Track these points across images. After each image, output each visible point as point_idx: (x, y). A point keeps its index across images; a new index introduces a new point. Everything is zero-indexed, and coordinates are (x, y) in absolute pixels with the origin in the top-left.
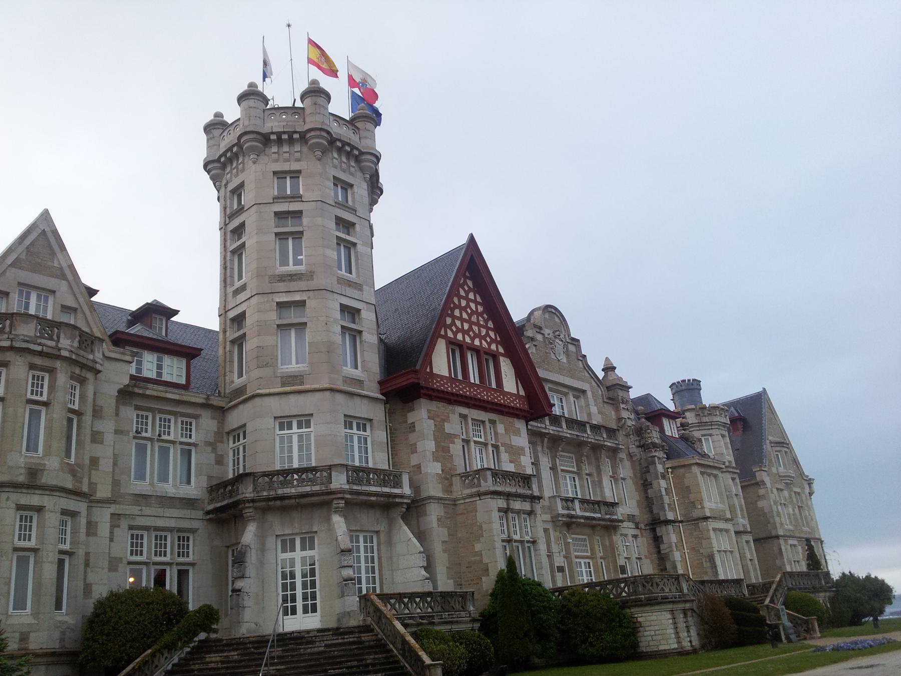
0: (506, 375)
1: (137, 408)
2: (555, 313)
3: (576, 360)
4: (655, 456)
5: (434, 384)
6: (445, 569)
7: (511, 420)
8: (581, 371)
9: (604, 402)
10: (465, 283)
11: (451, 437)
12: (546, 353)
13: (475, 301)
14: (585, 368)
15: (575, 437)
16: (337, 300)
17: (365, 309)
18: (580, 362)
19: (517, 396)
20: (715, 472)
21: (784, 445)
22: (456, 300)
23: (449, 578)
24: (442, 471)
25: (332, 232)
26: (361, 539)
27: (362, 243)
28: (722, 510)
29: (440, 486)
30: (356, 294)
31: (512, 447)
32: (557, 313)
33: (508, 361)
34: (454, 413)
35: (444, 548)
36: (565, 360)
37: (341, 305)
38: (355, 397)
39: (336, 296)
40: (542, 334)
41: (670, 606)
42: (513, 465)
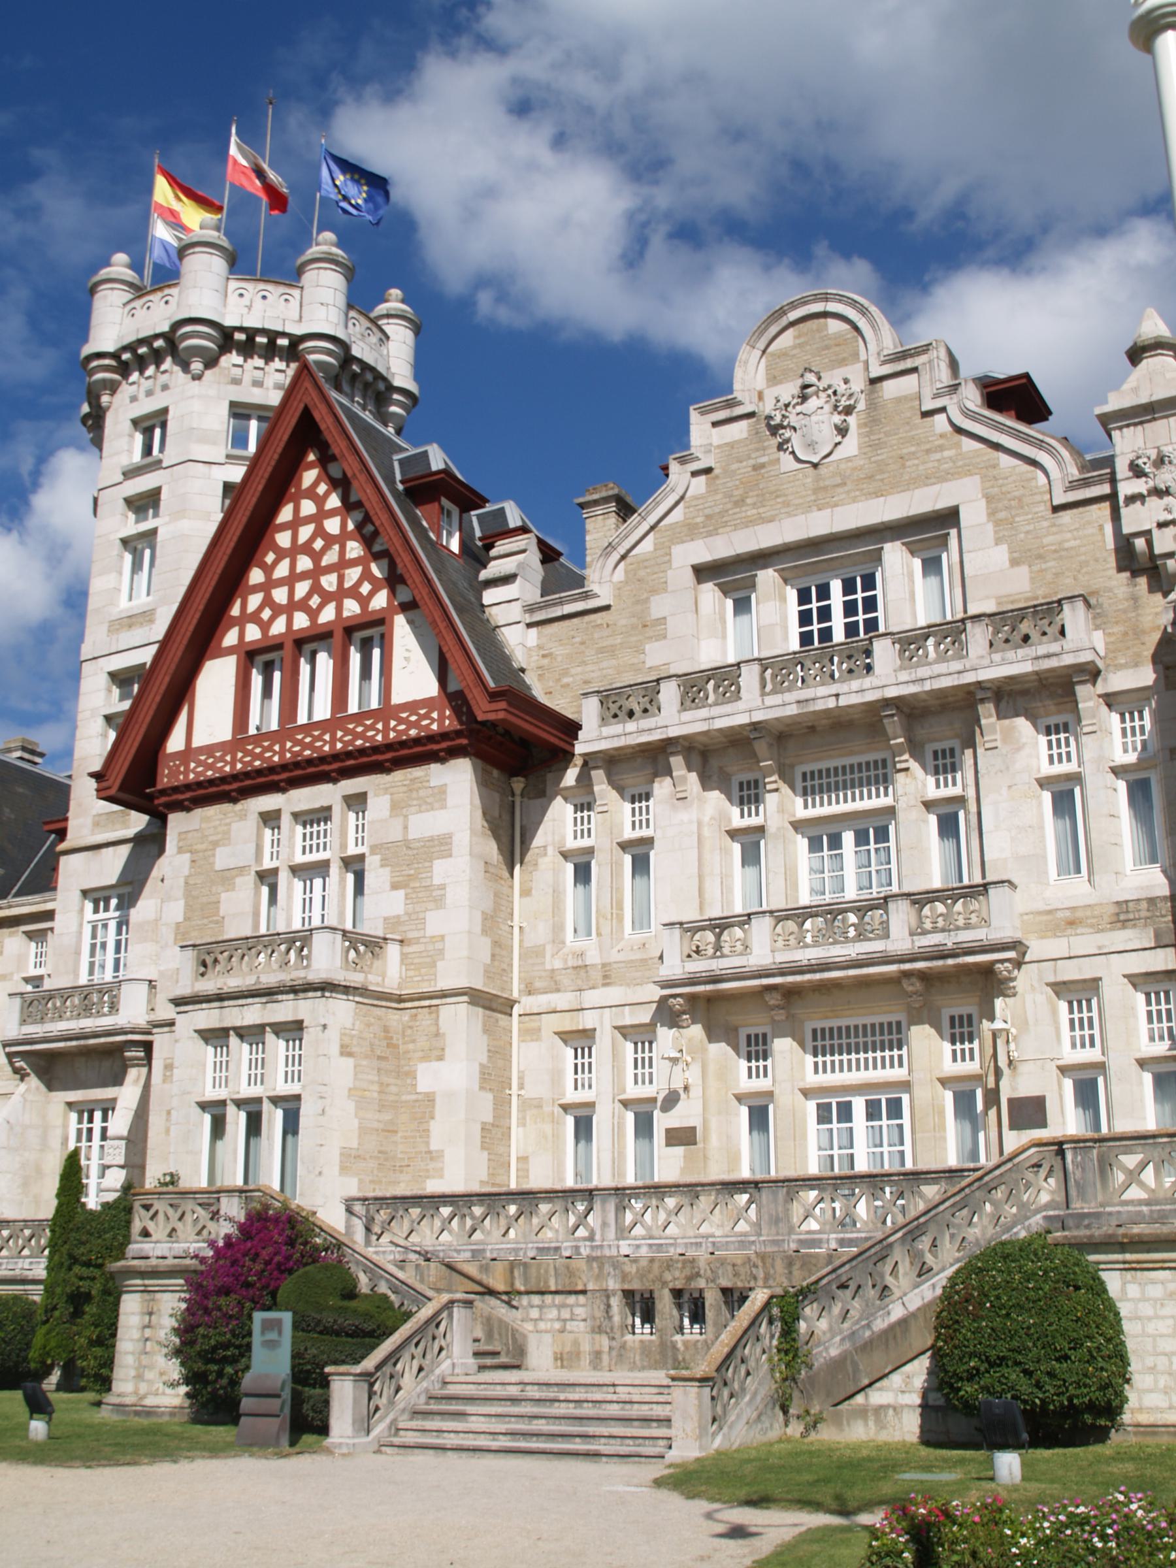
0: (407, 659)
2: (825, 315)
3: (917, 419)
7: (417, 772)
8: (941, 448)
9: (1056, 509)
11: (227, 877)
12: (756, 468)
14: (959, 430)
15: (792, 710)
18: (940, 419)
27: (167, 519)
31: (407, 843)
32: (833, 307)
34: (243, 816)
40: (751, 415)
42: (401, 893)
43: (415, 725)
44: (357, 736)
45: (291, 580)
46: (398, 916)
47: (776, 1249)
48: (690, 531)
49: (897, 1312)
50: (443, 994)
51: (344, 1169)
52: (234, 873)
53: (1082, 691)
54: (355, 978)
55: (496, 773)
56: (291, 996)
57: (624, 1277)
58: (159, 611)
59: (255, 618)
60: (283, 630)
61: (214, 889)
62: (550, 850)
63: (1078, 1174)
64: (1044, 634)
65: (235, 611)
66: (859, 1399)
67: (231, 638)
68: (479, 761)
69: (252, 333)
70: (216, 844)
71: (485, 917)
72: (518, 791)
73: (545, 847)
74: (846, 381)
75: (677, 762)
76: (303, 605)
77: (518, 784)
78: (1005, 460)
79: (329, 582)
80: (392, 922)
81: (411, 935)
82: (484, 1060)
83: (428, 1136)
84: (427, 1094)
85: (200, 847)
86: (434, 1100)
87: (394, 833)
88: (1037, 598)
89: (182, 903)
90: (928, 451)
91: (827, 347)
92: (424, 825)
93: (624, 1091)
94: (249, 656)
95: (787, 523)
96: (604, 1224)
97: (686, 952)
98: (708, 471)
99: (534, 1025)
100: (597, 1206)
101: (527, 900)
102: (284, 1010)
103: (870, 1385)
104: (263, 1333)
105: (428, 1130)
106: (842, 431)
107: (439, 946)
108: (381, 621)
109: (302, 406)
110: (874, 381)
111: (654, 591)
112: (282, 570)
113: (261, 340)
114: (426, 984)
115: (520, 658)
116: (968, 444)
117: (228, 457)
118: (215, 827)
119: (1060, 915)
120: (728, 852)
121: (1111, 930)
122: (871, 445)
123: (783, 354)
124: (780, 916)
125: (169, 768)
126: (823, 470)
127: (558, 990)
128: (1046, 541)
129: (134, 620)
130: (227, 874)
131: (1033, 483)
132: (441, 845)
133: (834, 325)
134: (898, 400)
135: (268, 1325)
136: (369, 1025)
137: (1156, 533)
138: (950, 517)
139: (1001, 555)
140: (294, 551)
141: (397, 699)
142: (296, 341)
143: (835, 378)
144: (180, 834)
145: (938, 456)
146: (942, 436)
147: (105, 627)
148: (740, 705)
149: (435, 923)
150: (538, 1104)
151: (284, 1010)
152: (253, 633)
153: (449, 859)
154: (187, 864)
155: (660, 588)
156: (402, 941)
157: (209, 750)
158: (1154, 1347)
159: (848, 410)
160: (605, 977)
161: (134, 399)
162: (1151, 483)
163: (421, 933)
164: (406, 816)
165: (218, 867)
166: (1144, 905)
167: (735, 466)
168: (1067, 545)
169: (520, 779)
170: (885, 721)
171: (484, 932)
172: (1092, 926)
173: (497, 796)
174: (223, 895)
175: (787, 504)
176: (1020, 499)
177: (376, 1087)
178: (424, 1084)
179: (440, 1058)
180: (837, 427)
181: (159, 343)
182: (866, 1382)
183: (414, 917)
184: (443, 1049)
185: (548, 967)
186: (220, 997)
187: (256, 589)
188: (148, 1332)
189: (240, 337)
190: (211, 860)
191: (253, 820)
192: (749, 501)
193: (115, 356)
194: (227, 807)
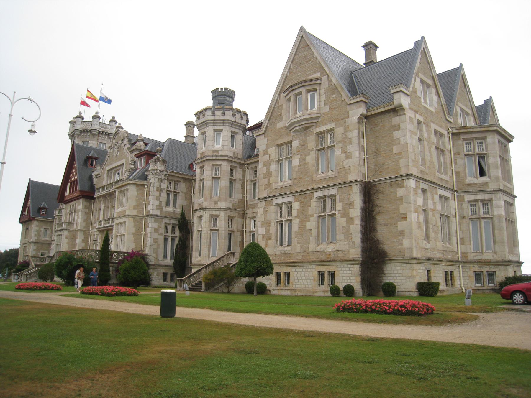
20: (126, 188)
21: (293, 88)
48: (108, 165)
55: (88, 200)
68: (85, 199)
69: (84, 130)
71: (84, 220)
77: (93, 201)
80: (76, 220)
82: (83, 238)
95: (114, 164)
98: (109, 156)
115: (94, 183)
122: (119, 153)
132: (79, 211)
138: (123, 164)
142: (90, 130)
148: (105, 191)
171: (84, 222)
173: (89, 203)
189: (82, 131)
193: (71, 134)
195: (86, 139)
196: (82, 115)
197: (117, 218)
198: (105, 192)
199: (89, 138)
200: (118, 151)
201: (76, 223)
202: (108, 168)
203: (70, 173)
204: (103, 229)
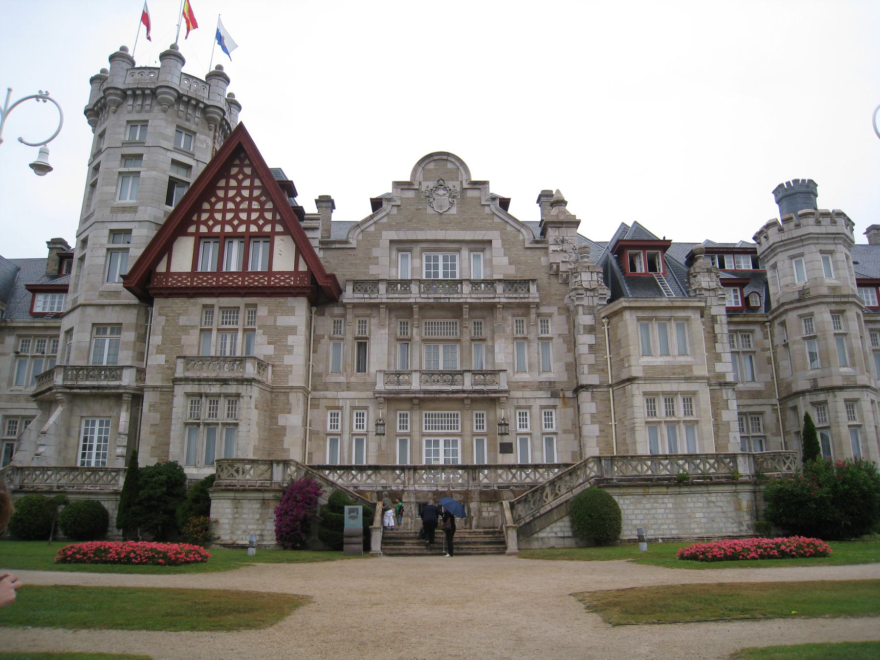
0: (280, 254)
1: (19, 336)
2: (447, 160)
4: (578, 305)
5: (167, 281)
6: (150, 448)
7: (282, 300)
8: (487, 219)
10: (241, 171)
11: (185, 329)
12: (417, 209)
13: (251, 188)
14: (494, 214)
16: (106, 227)
17: (137, 227)
18: (487, 208)
19: (296, 273)
22: (221, 193)
23: (152, 456)
24: (166, 361)
25: (114, 170)
26: (97, 423)
28: (685, 366)
29: (160, 376)
30: (128, 216)
31: (276, 327)
33: (288, 239)
35: (152, 430)
36: (454, 211)
37: (111, 231)
38: (107, 307)
39: (106, 224)
41: (232, 495)
43: (284, 281)
44: (255, 281)
45: (224, 211)
46: (271, 355)
47: (475, 489)
48: (389, 227)
49: (548, 508)
50: (292, 388)
51: (254, 454)
52: (189, 327)
53: (533, 311)
54: (260, 378)
56: (235, 383)
57: (417, 498)
58: (139, 208)
59: (205, 223)
60: (219, 231)
61: (178, 333)
62: (326, 337)
63: (606, 467)
64: (510, 290)
65: (195, 218)
66: (536, 535)
67: (192, 229)
70: (180, 314)
72: (313, 312)
73: (324, 335)
74: (454, 187)
75: (382, 311)
76: (230, 222)
77: (314, 309)
78: (509, 228)
79: (243, 216)
81: (276, 363)
83: (283, 443)
84: (283, 426)
85: (171, 314)
86: (286, 429)
87: (270, 322)
88: (517, 277)
89: (161, 337)
90: (482, 219)
91: (447, 172)
92: (283, 321)
93: (352, 431)
94: (200, 238)
95: (428, 232)
96: (409, 479)
97: (386, 381)
98: (398, 206)
99: (317, 403)
100: (406, 472)
101: (315, 354)
102: (232, 389)
103: (539, 531)
104: (349, 513)
105: (283, 441)
106: (452, 204)
107: (290, 369)
108: (269, 238)
109: (238, 142)
110: (464, 190)
111: (375, 247)
112: (220, 206)
113: (194, 102)
114: (283, 383)
116: (496, 220)
117: (174, 148)
118: (180, 307)
119: (520, 383)
120: (395, 347)
121: (537, 390)
123: (430, 170)
124: (422, 373)
125: (157, 279)
126: (443, 216)
127: (328, 391)
128: (522, 258)
129: (125, 209)
130: (185, 328)
131: (518, 238)
132: (293, 330)
133: (450, 166)
134: (472, 198)
135: (351, 511)
136: (262, 398)
137: (561, 264)
139: (505, 260)
140: (226, 200)
141: (275, 269)
143: (450, 184)
144: (160, 307)
145: (484, 221)
146: (487, 214)
147: (109, 209)
149: (288, 360)
150: (318, 433)
151: (232, 389)
152: (203, 229)
153: (295, 336)
154: (164, 321)
155: (378, 246)
156: (273, 365)
157: (180, 274)
158: (667, 516)
159: (454, 197)
160: (348, 387)
161: (129, 112)
162: (561, 248)
163: (281, 363)
164: (276, 317)
165: (181, 323)
166: (548, 383)
167: (409, 207)
168: (529, 261)
169: (315, 308)
170: (464, 309)
172: (530, 388)
174: (183, 336)
175: (428, 225)
176: (513, 242)
177: (263, 422)
178: (281, 422)
179: (289, 413)
180: (450, 202)
181: (148, 92)
182: (538, 530)
183: (279, 356)
184: (291, 409)
185: (323, 381)
186: (199, 380)
187: (205, 211)
188: (237, 516)
189: (185, 99)
190: (177, 321)
191: (200, 307)
192: (414, 221)
193: (124, 92)
194: (185, 299)
195: (187, 125)
196: (130, 53)
197: (645, 379)
198: (398, 297)
199: (197, 124)
200: (452, 204)
201: (273, 365)
202: (394, 235)
203: (201, 211)
204: (422, 395)
